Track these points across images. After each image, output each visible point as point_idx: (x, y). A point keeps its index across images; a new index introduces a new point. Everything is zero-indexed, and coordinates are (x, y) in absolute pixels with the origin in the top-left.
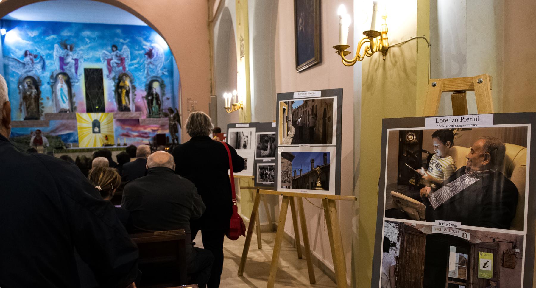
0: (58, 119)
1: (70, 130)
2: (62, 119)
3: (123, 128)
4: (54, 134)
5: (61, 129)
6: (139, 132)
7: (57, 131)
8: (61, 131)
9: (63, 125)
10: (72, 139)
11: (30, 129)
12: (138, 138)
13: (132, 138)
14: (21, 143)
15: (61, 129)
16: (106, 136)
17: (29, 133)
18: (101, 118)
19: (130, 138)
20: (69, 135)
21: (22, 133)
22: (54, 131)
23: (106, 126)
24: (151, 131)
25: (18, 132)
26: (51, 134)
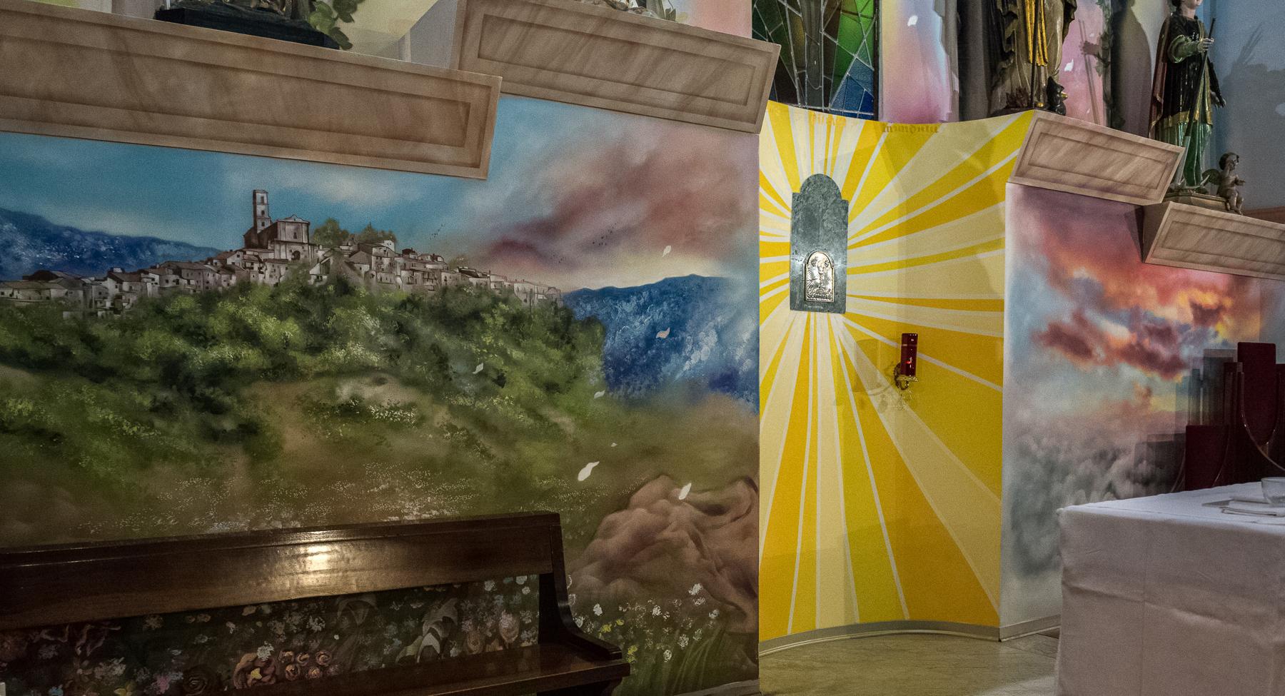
0: (582, 98)
1: (692, 240)
2: (626, 105)
3: (1057, 278)
4: (531, 283)
5: (609, 219)
6: (1133, 318)
7: (565, 246)
8: (604, 243)
9: (630, 180)
10: (701, 353)
11: (242, 177)
12: (1132, 373)
13: (1101, 371)
14: (99, 375)
15: (609, 219)
16: (909, 343)
17: (229, 238)
18: (860, 158)
19: (1086, 366)
20: (679, 298)
21: (120, 225)
22: (533, 239)
23: (890, 250)
24: (1189, 316)
25: (60, 216)
26: (500, 276)
